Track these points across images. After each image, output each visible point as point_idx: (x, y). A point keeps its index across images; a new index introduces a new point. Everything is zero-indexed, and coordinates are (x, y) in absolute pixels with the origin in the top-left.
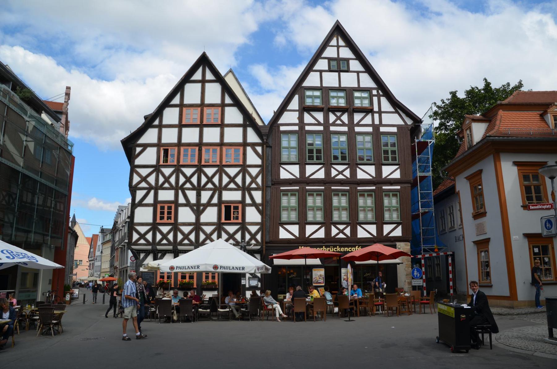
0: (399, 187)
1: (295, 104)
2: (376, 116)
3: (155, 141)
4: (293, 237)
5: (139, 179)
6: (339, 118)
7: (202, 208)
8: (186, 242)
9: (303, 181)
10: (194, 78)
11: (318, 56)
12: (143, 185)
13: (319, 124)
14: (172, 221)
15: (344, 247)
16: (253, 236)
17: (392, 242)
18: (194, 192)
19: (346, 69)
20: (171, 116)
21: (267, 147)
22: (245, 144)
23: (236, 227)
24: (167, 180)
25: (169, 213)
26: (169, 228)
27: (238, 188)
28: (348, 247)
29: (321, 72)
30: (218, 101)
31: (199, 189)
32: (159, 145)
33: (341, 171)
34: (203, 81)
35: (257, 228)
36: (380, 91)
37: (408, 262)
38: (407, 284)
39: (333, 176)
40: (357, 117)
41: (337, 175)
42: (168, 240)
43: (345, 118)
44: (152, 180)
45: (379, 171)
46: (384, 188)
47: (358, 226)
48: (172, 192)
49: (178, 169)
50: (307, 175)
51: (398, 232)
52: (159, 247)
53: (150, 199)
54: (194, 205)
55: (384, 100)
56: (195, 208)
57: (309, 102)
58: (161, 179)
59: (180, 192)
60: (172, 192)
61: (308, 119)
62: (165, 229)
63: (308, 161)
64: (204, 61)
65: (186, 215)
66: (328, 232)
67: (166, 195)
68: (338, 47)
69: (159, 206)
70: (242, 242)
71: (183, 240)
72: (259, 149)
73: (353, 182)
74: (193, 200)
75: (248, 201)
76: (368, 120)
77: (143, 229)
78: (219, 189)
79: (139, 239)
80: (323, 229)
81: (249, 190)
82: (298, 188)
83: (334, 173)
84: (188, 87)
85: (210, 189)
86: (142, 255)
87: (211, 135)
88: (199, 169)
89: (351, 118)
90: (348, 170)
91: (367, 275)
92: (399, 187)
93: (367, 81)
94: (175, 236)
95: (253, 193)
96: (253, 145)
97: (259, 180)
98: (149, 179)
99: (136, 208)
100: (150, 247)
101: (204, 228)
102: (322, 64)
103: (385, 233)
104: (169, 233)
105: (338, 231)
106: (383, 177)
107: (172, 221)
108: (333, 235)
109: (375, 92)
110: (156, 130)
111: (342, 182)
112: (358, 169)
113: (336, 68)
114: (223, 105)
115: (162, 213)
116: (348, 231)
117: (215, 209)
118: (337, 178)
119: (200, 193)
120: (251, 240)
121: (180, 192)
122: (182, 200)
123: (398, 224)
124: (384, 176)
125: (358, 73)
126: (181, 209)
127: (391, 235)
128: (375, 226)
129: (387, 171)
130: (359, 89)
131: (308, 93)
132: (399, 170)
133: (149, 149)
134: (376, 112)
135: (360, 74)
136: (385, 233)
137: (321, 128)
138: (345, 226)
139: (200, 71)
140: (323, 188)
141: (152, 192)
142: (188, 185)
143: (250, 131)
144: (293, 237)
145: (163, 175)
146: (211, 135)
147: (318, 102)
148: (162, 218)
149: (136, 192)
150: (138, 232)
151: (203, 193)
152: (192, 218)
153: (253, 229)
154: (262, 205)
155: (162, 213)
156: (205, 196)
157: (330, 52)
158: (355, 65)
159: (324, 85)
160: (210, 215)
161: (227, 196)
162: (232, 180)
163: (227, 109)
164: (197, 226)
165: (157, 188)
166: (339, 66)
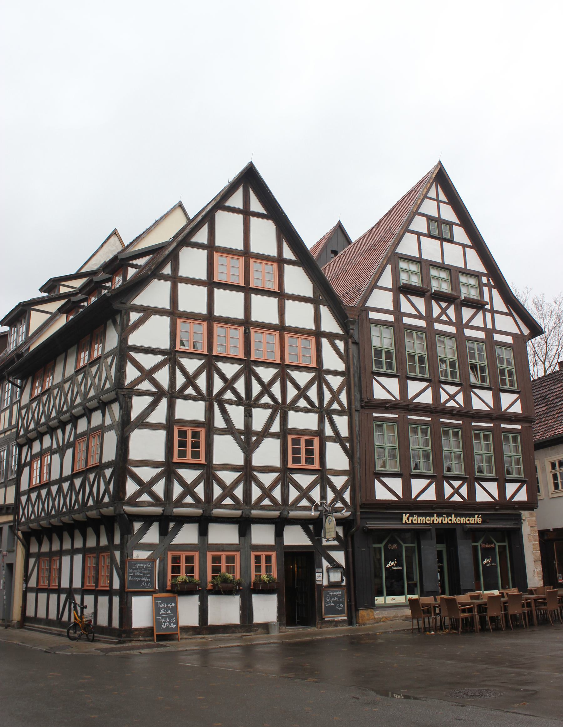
0: (519, 427)
3: (166, 304)
4: (396, 499)
5: (137, 374)
6: (444, 311)
7: (254, 439)
9: (404, 406)
10: (229, 203)
12: (146, 385)
13: (419, 316)
15: (461, 515)
17: (515, 509)
18: (241, 409)
19: (448, 237)
20: (193, 262)
21: (353, 343)
22: (318, 334)
24: (191, 380)
25: (196, 445)
27: (312, 409)
28: (465, 515)
29: (419, 234)
30: (273, 252)
31: (249, 404)
32: (173, 313)
33: (451, 396)
34: (246, 213)
36: (491, 280)
37: (535, 541)
38: (536, 574)
40: (467, 313)
41: (447, 401)
42: (195, 496)
43: (451, 312)
46: (503, 426)
47: (477, 485)
49: (210, 362)
50: (410, 397)
51: (522, 496)
52: (178, 511)
53: (159, 415)
54: (240, 432)
55: (495, 292)
56: (243, 438)
57: (404, 278)
58: (181, 380)
59: (216, 405)
61: (405, 307)
62: (189, 475)
63: (409, 374)
64: (250, 179)
65: (227, 451)
66: (440, 491)
67: (190, 410)
68: (438, 201)
70: (321, 503)
71: (222, 497)
72: (340, 344)
73: (467, 414)
74: (239, 424)
75: (329, 432)
76: (478, 321)
77: (146, 474)
78: (282, 408)
79: (138, 494)
80: (433, 486)
81: (330, 413)
82: (397, 416)
83: (444, 397)
84: (221, 217)
85: (266, 406)
86: (137, 526)
87: (264, 310)
88: (248, 367)
89: (459, 315)
91: (391, 564)
92: (519, 427)
93: (475, 263)
94: (208, 491)
96: (331, 337)
97: (343, 397)
98: (156, 376)
101: (260, 476)
103: (508, 497)
104: (196, 482)
109: (484, 280)
110: (166, 286)
111: (455, 412)
113: (436, 233)
114: (280, 261)
115: (182, 444)
116: (464, 491)
117: (276, 443)
119: (251, 411)
120: (334, 500)
121: (216, 405)
122: (219, 422)
123: (523, 482)
125: (464, 246)
126: (218, 439)
128: (496, 483)
131: (403, 265)
132: (519, 402)
133: (154, 318)
134: (488, 311)
136: (508, 497)
137: (422, 323)
138: (460, 482)
139: (240, 192)
141: (164, 402)
142: (229, 395)
143: (325, 311)
144: (396, 499)
145: (184, 372)
147: (415, 281)
148: (182, 454)
149: (131, 398)
151: (255, 411)
153: (339, 481)
154: (351, 439)
155: (182, 444)
156: (260, 417)
158: (460, 234)
159: (423, 257)
160: (268, 453)
162: (302, 393)
163: (287, 268)
164: (248, 472)
165: (174, 395)
166: (439, 231)
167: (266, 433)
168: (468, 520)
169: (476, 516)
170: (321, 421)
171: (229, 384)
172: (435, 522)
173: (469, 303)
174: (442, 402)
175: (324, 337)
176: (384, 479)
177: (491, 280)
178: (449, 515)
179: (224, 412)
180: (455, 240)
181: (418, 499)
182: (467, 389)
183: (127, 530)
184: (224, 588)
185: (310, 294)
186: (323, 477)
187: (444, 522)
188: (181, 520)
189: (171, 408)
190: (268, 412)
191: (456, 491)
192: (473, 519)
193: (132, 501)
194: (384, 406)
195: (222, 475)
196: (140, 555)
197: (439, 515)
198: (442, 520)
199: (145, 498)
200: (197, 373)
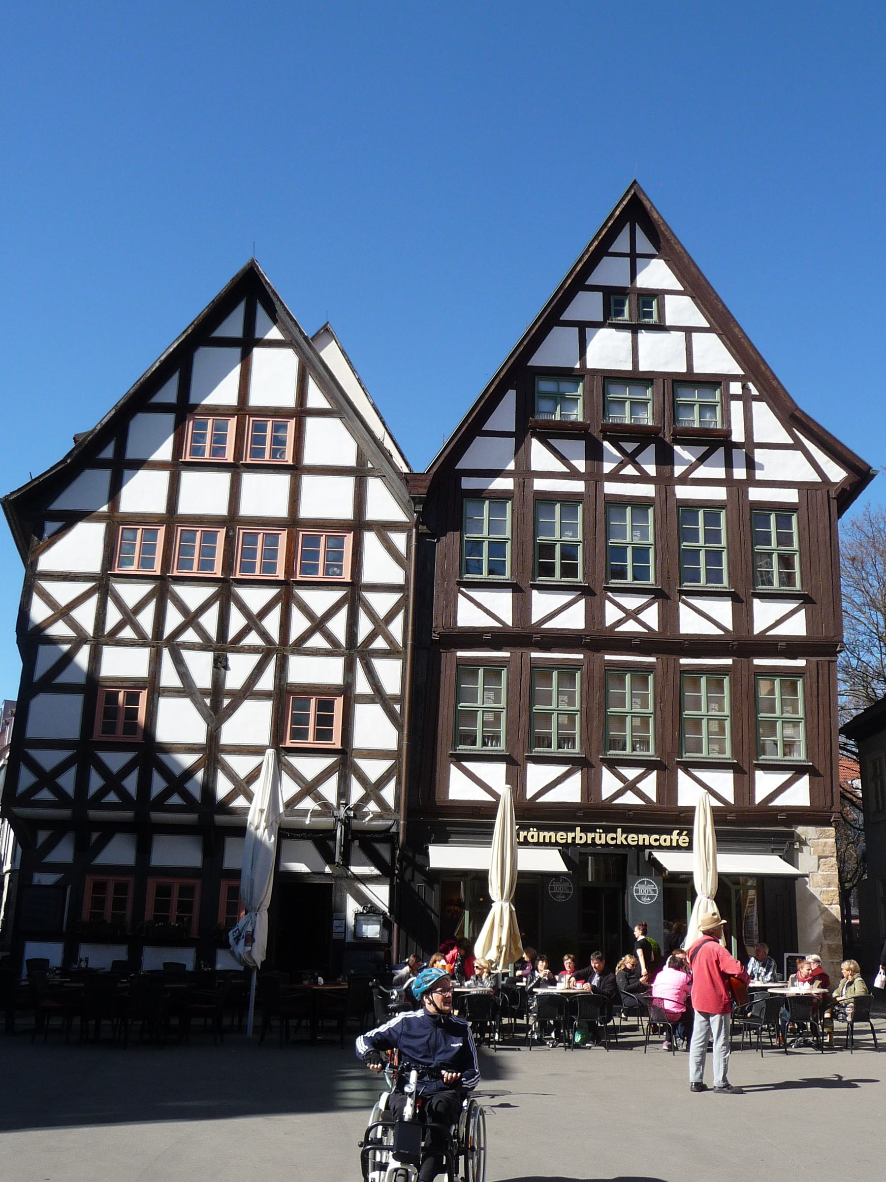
0: (801, 663)
1: (505, 416)
2: (739, 455)
7: (226, 702)
8: (176, 799)
9: (522, 636)
11: (578, 282)
13: (573, 474)
15: (638, 831)
16: (373, 790)
19: (655, 319)
23: (325, 762)
24: (129, 617)
28: (650, 832)
30: (289, 401)
31: (221, 648)
33: (631, 613)
35: (384, 765)
36: (751, 385)
39: (609, 621)
42: (122, 793)
44: (86, 616)
45: (743, 614)
48: (143, 654)
50: (535, 619)
51: (799, 795)
52: (94, 814)
54: (204, 692)
55: (761, 409)
56: (208, 701)
58: (113, 616)
59: (166, 653)
60: (143, 654)
66: (591, 786)
70: (339, 804)
72: (399, 540)
73: (668, 644)
74: (203, 678)
75: (362, 686)
77: (48, 759)
78: (278, 651)
83: (612, 614)
86: (42, 836)
87: (265, 495)
90: (655, 607)
93: (714, 356)
95: (379, 664)
96: (383, 528)
97: (396, 628)
98: (75, 614)
99: (35, 694)
101: (232, 761)
102: (588, 306)
103: (759, 798)
104: (126, 771)
105: (621, 785)
106: (756, 631)
108: (606, 794)
112: (681, 605)
114: (301, 412)
116: (649, 785)
117: (265, 708)
118: (622, 628)
120: (364, 800)
121: (166, 653)
122: (169, 677)
123: (799, 771)
124: (758, 629)
125: (689, 331)
126: (164, 704)
127: (778, 802)
129: (765, 615)
130: (690, 380)
132: (803, 612)
134: (738, 446)
135: (695, 335)
136: (759, 798)
138: (638, 771)
140: (581, 656)
142: (190, 636)
146: (265, 495)
151: (233, 659)
153: (374, 769)
156: (240, 668)
157: (611, 272)
158: (681, 310)
160: (251, 723)
161: (304, 670)
162: (319, 625)
163: (311, 423)
167: (248, 692)
168: (656, 840)
169: (676, 832)
170: (349, 669)
171: (191, 619)
172: (578, 841)
173: (689, 438)
174: (608, 624)
175: (370, 530)
176: (465, 764)
177: (751, 385)
178: (607, 830)
179: (179, 662)
180: (669, 322)
181: (538, 801)
182: (665, 597)
184: (101, 935)
185: (350, 461)
186: (345, 761)
187: (598, 841)
188: (109, 830)
190: (256, 658)
191: (631, 786)
192: (668, 837)
194: (475, 638)
197: (585, 830)
198: (593, 839)
199: (45, 795)
200: (140, 606)
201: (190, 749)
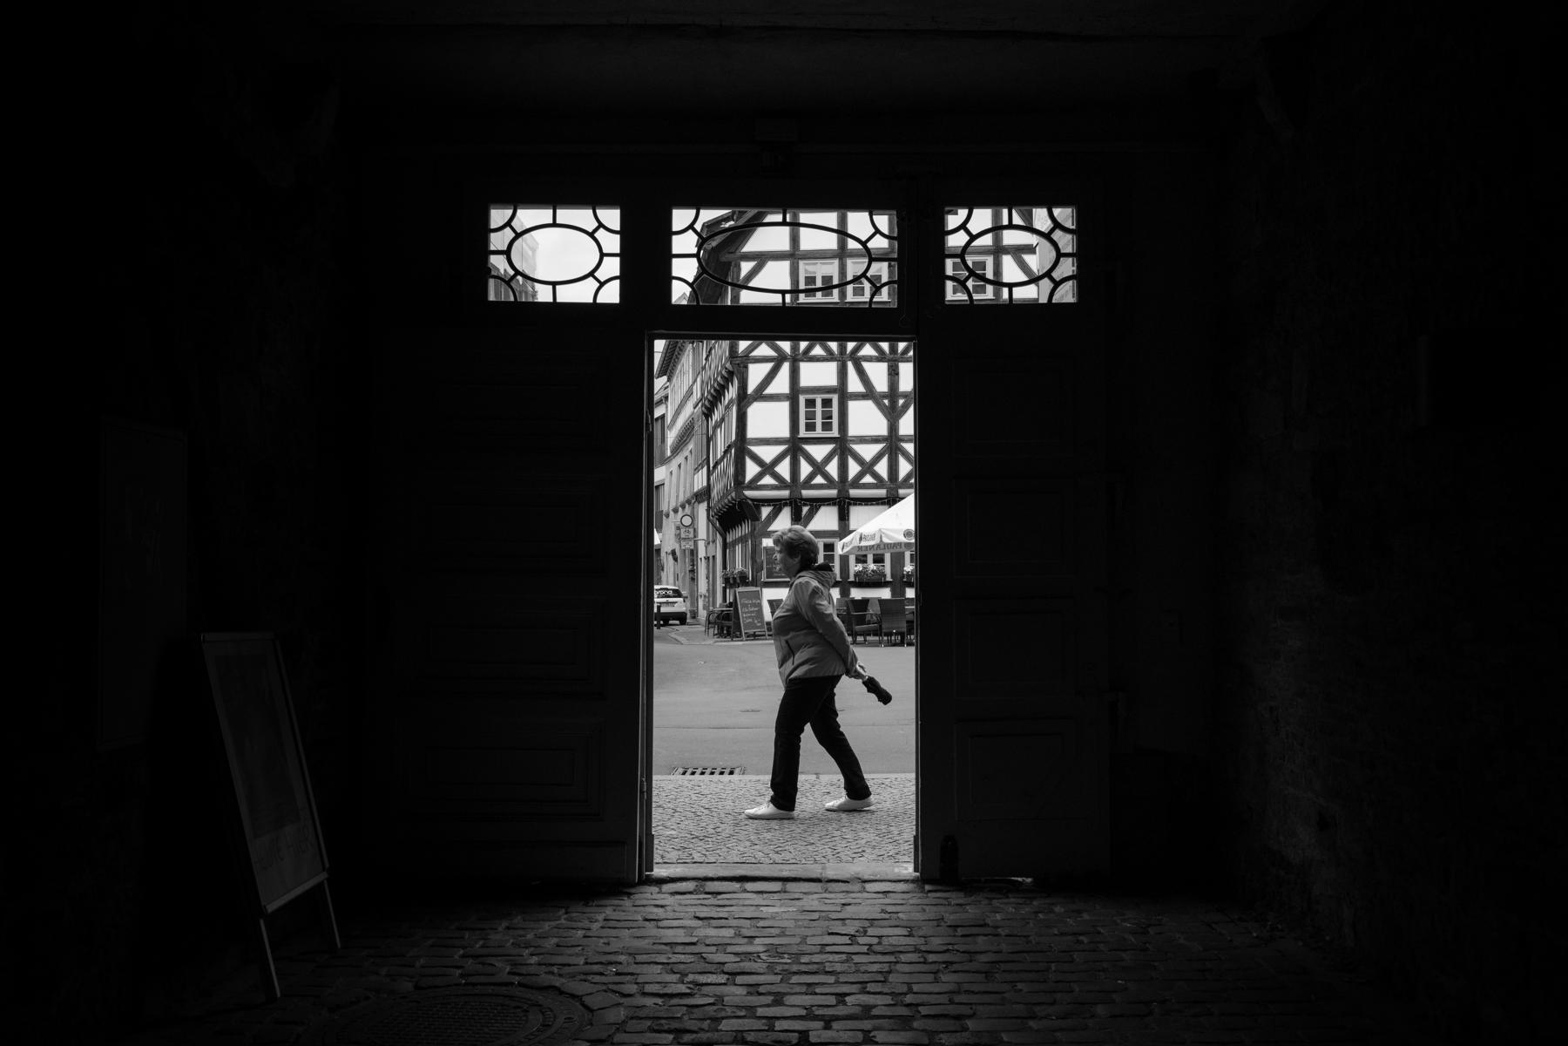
7: (901, 402)
8: (868, 479)
14: (835, 433)
18: (884, 366)
26: (828, 448)
32: (794, 255)
42: (826, 476)
48: (832, 367)
52: (806, 493)
53: (781, 384)
54: (884, 396)
59: (850, 365)
60: (832, 367)
62: (819, 452)
69: (802, 399)
71: (861, 475)
74: (881, 385)
77: (768, 453)
79: (760, 476)
86: (765, 511)
94: (843, 468)
99: (750, 404)
100: (785, 493)
104: (828, 459)
107: (835, 433)
115: (810, 416)
121: (850, 365)
122: (855, 385)
126: (853, 406)
133: (771, 266)
141: (786, 367)
148: (810, 427)
149: (746, 367)
150: (758, 460)
152: (880, 426)
155: (810, 416)
183: (756, 517)
189: (794, 375)
193: (754, 484)
195: (859, 449)
196: (768, 542)
201: (875, 440)
